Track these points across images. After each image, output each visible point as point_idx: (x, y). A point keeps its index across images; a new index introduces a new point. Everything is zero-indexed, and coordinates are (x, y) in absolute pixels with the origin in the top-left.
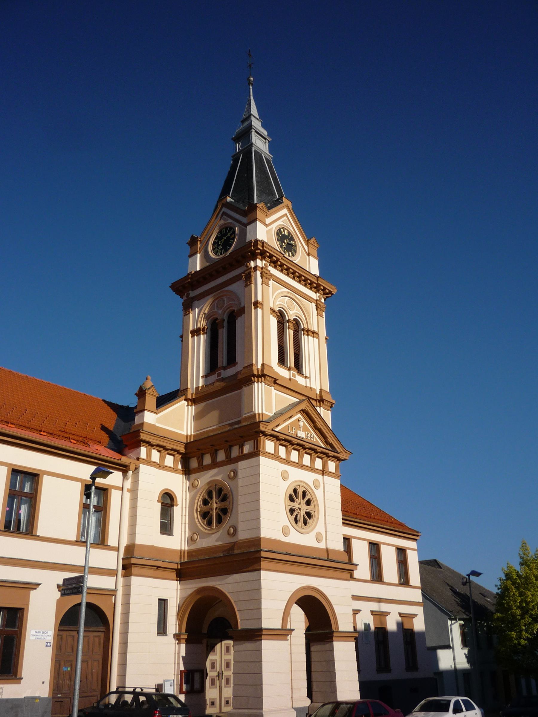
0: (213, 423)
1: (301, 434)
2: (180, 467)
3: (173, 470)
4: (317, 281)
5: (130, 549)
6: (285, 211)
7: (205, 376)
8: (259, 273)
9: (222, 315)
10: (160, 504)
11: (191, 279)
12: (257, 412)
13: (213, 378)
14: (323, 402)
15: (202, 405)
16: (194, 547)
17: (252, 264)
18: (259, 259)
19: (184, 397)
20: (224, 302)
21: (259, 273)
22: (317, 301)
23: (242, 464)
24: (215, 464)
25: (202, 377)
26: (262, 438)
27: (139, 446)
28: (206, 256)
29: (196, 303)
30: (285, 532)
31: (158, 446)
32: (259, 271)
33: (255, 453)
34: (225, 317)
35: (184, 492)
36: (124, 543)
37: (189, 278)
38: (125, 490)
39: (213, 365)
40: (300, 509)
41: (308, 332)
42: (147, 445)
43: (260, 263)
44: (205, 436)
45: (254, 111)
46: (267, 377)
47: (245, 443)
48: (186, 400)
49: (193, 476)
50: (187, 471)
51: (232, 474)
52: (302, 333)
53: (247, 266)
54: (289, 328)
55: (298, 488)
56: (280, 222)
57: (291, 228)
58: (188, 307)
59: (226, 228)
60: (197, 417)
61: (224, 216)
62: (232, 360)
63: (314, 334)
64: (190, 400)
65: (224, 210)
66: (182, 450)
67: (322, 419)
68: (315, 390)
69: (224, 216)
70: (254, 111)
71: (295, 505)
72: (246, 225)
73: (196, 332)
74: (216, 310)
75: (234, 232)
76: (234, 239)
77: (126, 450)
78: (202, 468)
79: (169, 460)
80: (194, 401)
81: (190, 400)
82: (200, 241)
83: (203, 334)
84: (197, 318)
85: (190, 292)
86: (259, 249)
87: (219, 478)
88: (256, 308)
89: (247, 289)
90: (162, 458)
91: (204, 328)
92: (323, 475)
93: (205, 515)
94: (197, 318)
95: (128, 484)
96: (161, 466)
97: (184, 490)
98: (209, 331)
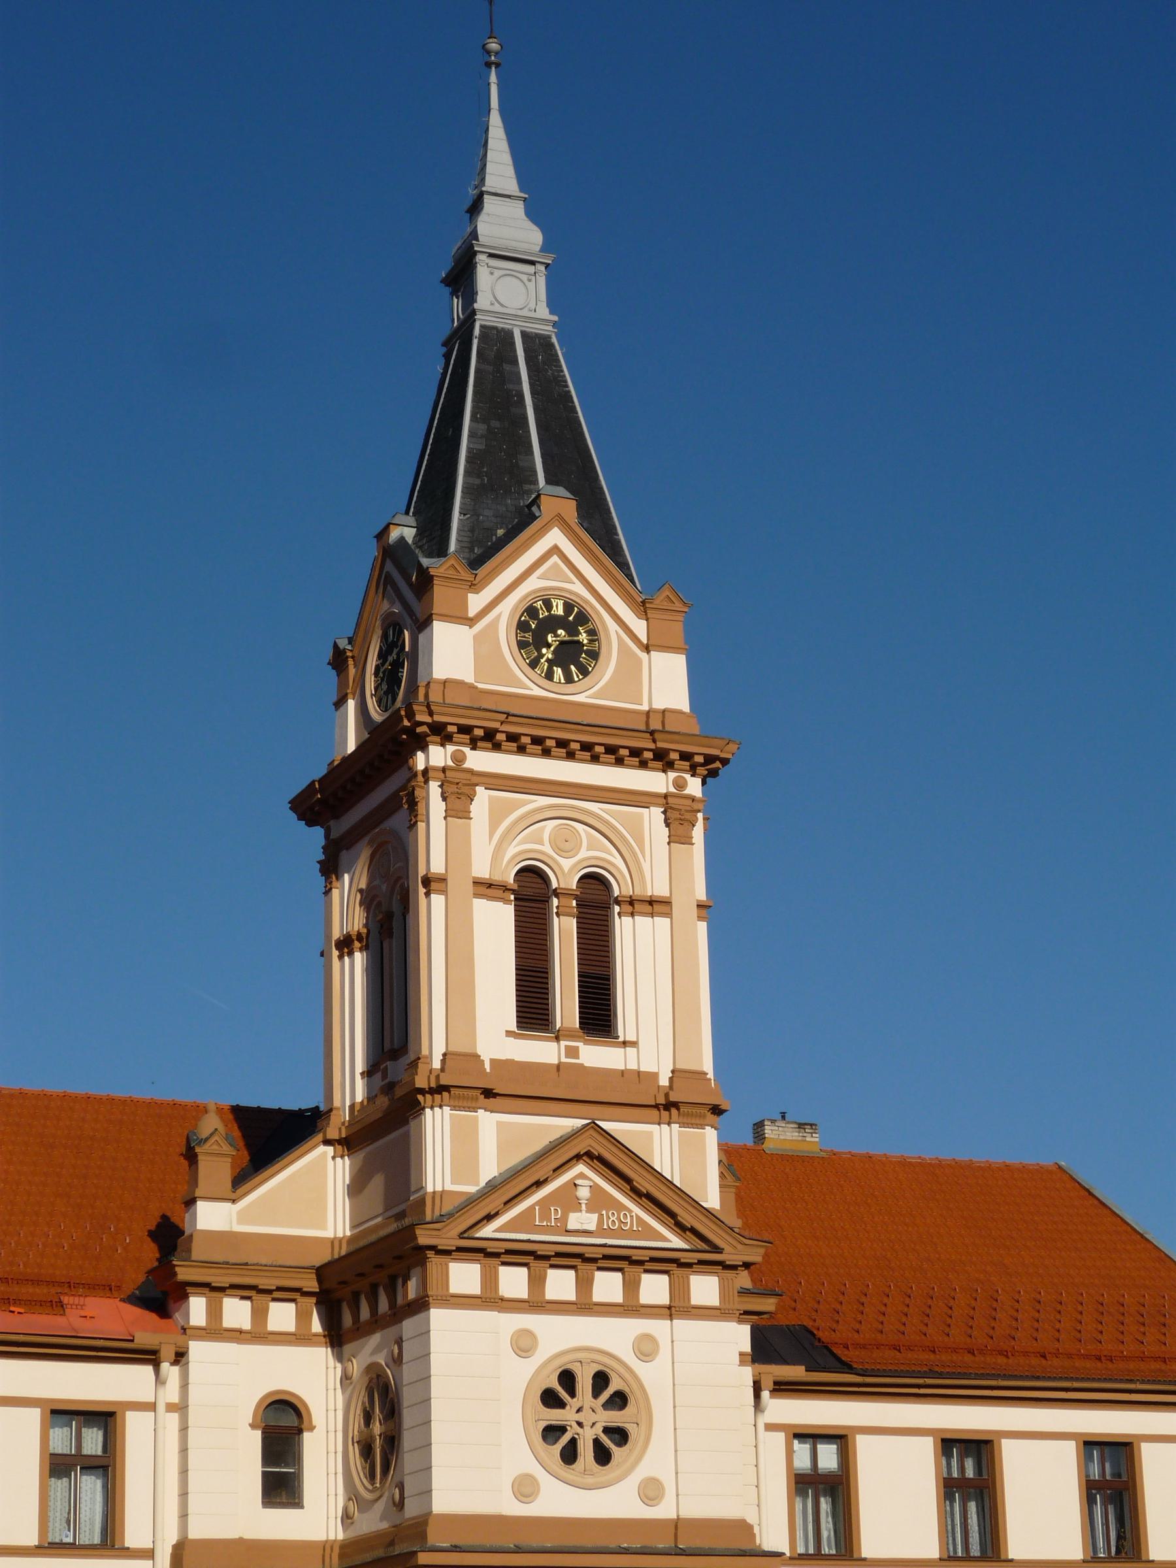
1: (583, 1220)
2: (316, 1326)
3: (300, 1338)
4: (654, 741)
5: (179, 1551)
6: (555, 537)
7: (368, 1074)
8: (434, 788)
10: (259, 1432)
11: (321, 791)
12: (430, 1189)
14: (678, 1109)
15: (360, 1155)
16: (354, 1533)
18: (434, 743)
19: (320, 1137)
21: (434, 788)
25: (362, 1074)
26: (434, 1261)
27: (185, 1297)
30: (525, 1488)
31: (233, 1287)
32: (436, 779)
35: (331, 1392)
36: (170, 1537)
37: (316, 792)
38: (161, 1407)
40: (580, 1424)
41: (633, 905)
42: (206, 1290)
43: (437, 755)
44: (373, 1238)
45: (500, 170)
46: (453, 1091)
48: (327, 1142)
49: (348, 1348)
50: (336, 1338)
52: (617, 909)
53: (410, 769)
54: (558, 914)
55: (576, 1369)
56: (533, 584)
57: (578, 588)
58: (330, 868)
63: (655, 906)
64: (340, 1142)
66: (312, 1285)
68: (655, 1076)
70: (500, 170)
73: (345, 945)
77: (171, 1305)
78: (361, 1331)
79: (282, 1316)
81: (340, 1142)
82: (353, 657)
83: (361, 950)
86: (422, 724)
90: (260, 1315)
93: (367, 1450)
95: (171, 1392)
96: (259, 1335)
97: (331, 1386)
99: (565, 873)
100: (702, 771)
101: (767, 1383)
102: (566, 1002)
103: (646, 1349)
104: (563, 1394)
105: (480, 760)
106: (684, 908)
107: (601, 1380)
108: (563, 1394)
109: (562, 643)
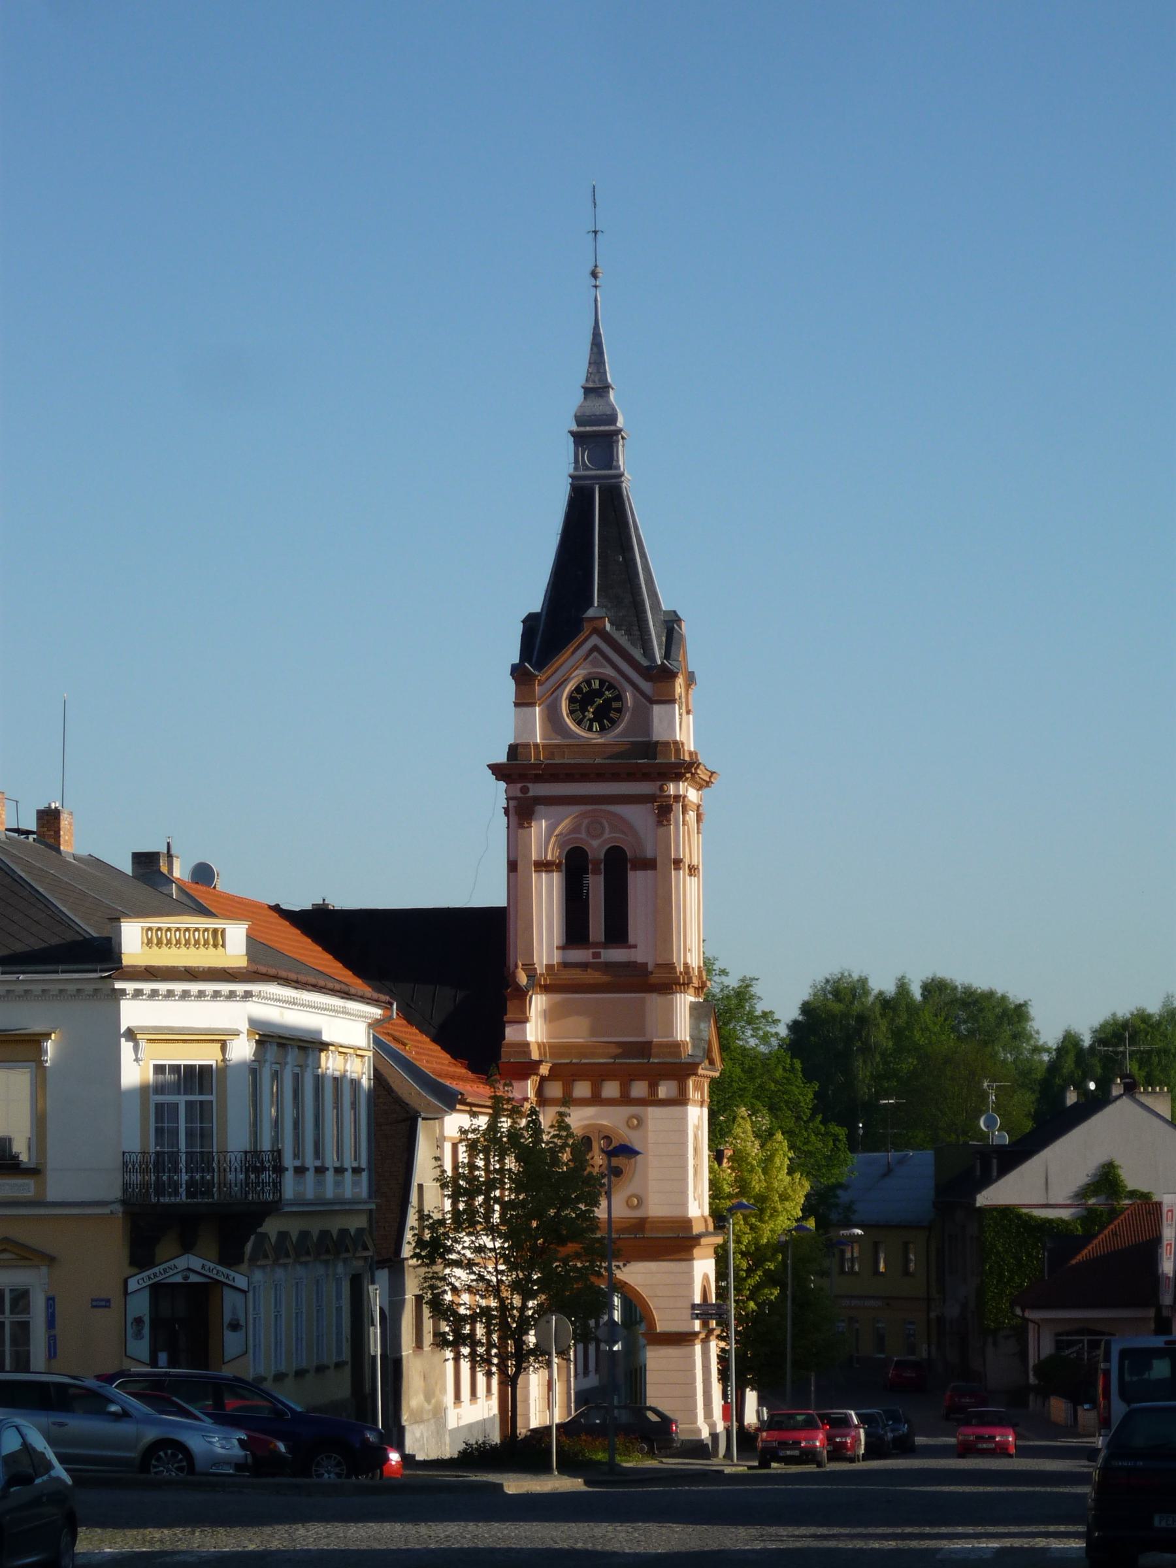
0: (577, 1031)
9: (596, 848)
13: (579, 955)
15: (558, 997)
17: (672, 789)
20: (603, 828)
22: (699, 806)
23: (653, 1112)
24: (596, 1100)
25: (558, 948)
28: (552, 717)
29: (541, 809)
33: (681, 1100)
34: (602, 856)
39: (575, 930)
47: (662, 1083)
51: (635, 1122)
53: (661, 789)
59: (602, 682)
60: (550, 1015)
61: (595, 654)
62: (617, 933)
64: (541, 986)
65: (595, 640)
69: (595, 654)
72: (653, 702)
73: (543, 866)
74: (583, 836)
75: (619, 698)
76: (619, 710)
80: (546, 989)
84: (543, 836)
85: (530, 785)
87: (605, 1122)
88: (677, 868)
89: (661, 830)
91: (560, 862)
92: (702, 1106)
94: (543, 836)
98: (564, 868)
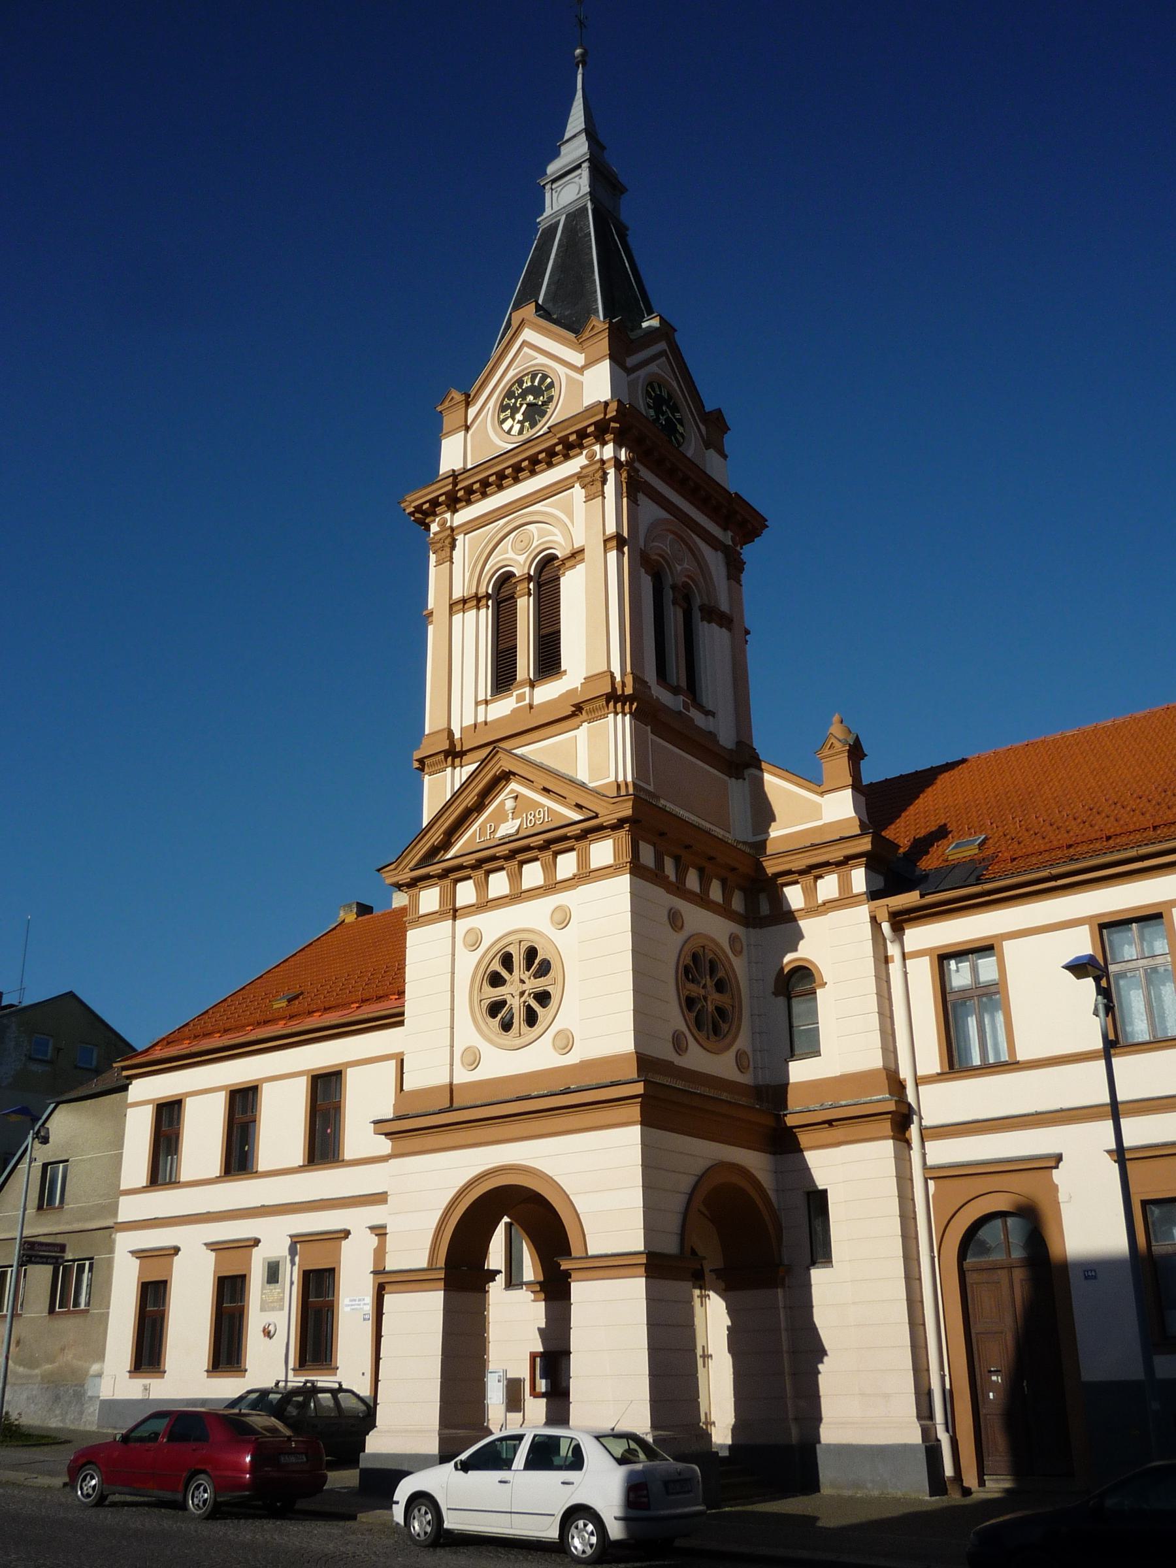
1: (508, 828)
6: (528, 334)
45: (576, 120)
55: (512, 949)
56: (511, 373)
57: (542, 359)
67: (456, 796)
70: (576, 120)
71: (535, 984)
99: (520, 563)
100: (609, 437)
101: (883, 916)
102: (525, 663)
103: (563, 919)
104: (504, 973)
105: (464, 515)
106: (595, 549)
107: (531, 953)
108: (504, 973)
109: (529, 405)
